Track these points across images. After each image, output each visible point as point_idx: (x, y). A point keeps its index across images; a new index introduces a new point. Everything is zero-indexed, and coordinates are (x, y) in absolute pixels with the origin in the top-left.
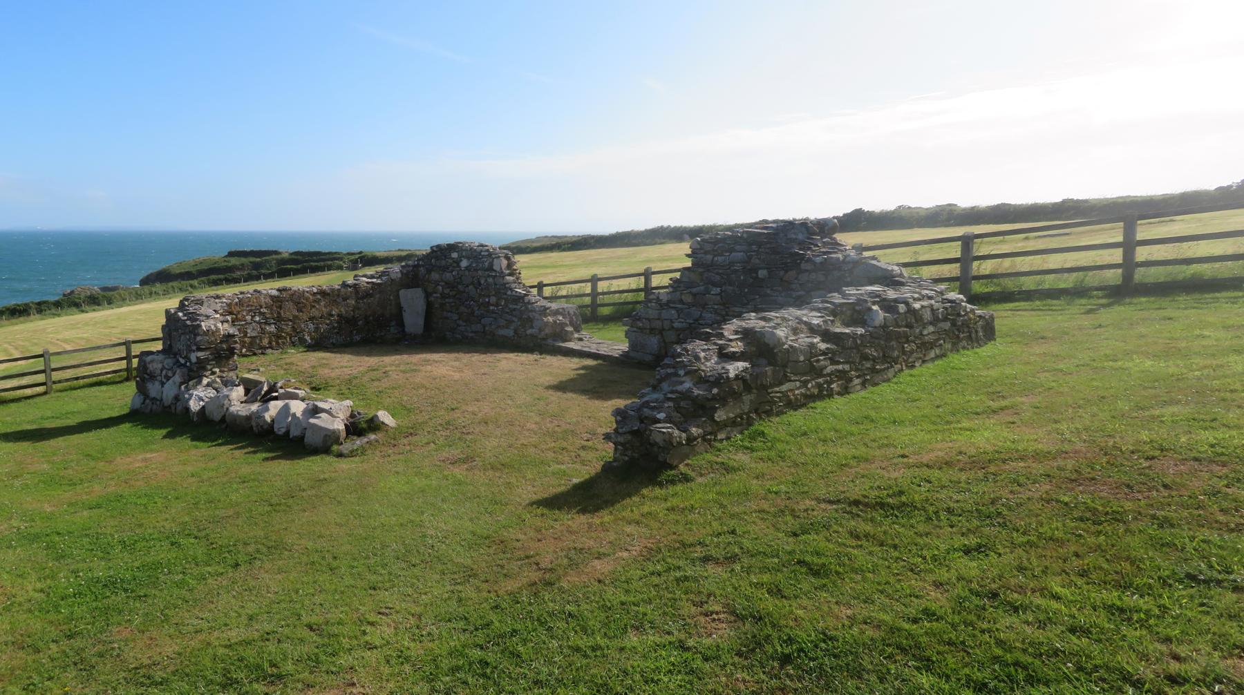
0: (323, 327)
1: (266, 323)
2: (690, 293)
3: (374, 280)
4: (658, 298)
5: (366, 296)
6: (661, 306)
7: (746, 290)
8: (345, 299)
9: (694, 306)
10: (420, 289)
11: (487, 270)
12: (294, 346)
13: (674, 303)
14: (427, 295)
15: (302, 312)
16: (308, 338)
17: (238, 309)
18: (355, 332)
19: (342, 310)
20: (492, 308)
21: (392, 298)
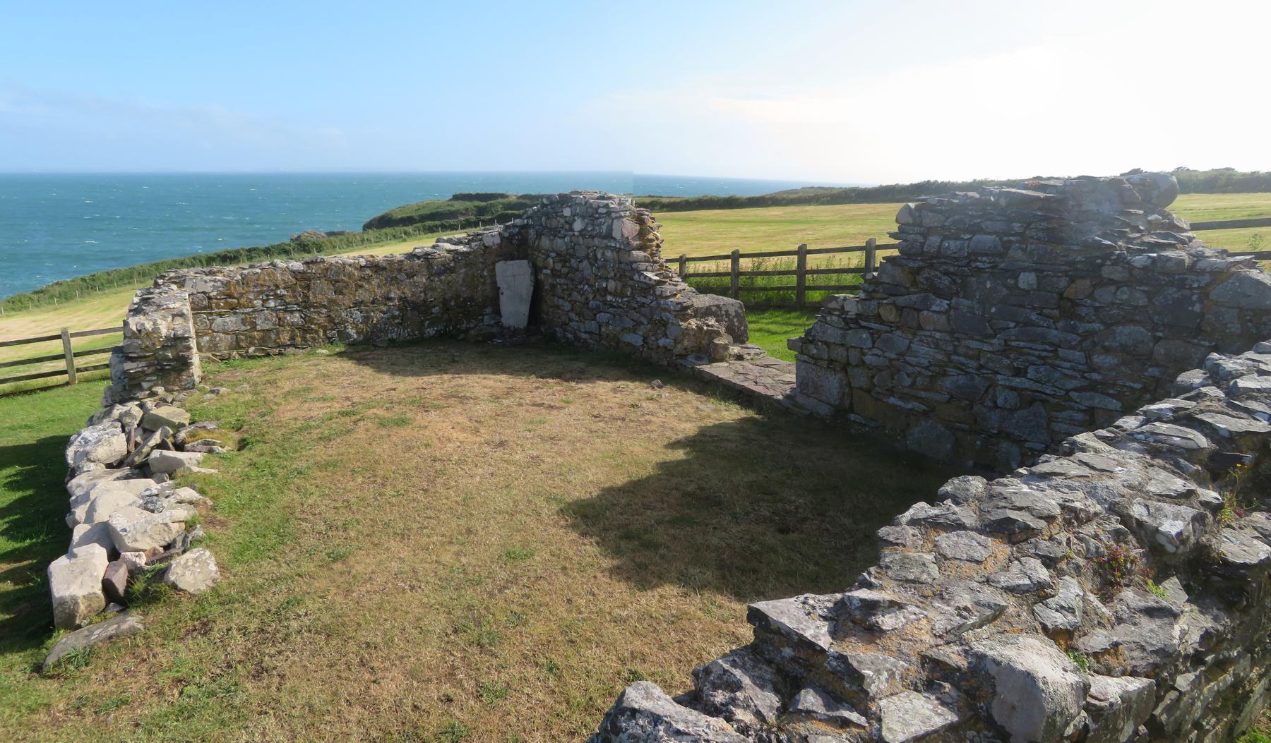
0: (376, 317)
1: (285, 311)
2: (894, 304)
4: (843, 307)
5: (445, 272)
6: (847, 324)
7: (993, 310)
8: (410, 276)
9: (898, 328)
10: (525, 262)
11: (605, 237)
12: (332, 343)
13: (867, 319)
14: (536, 270)
15: (341, 293)
16: (352, 331)
17: (240, 290)
19: (406, 290)
20: (609, 298)
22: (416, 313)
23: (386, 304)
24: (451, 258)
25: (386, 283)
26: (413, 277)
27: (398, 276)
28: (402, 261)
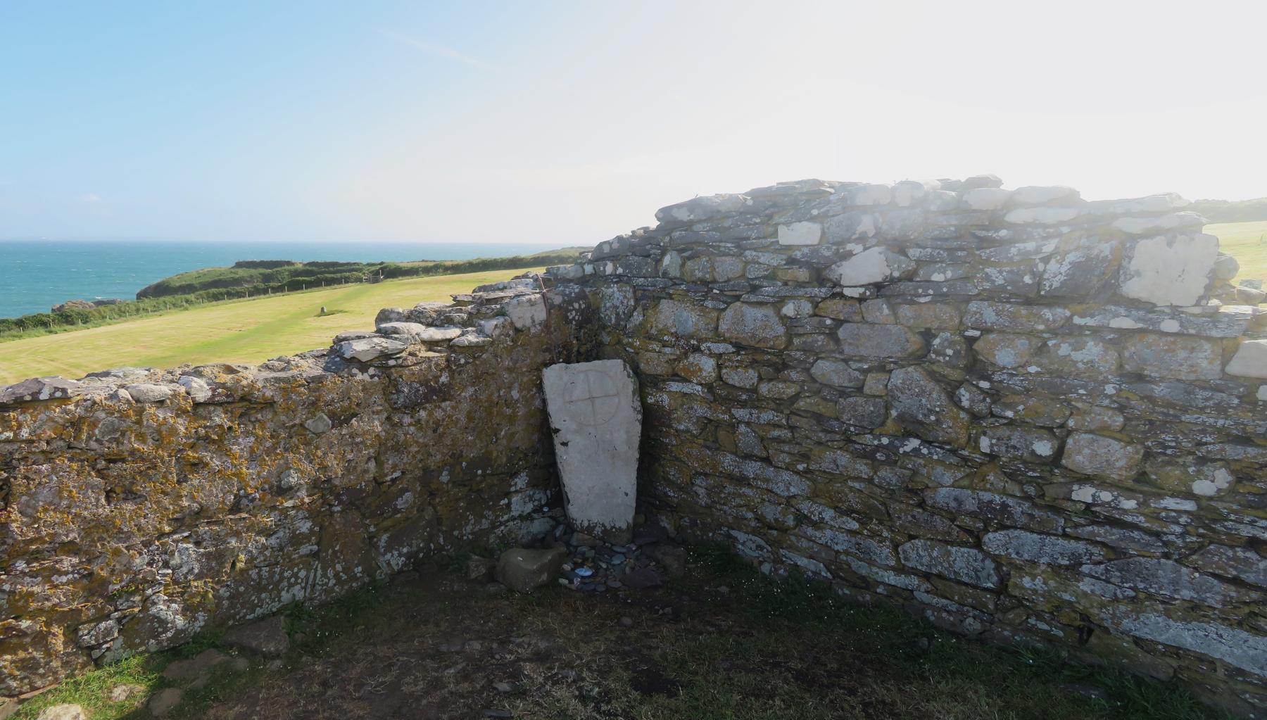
3: (453, 333)
5: (427, 398)
8: (339, 419)
15: (130, 495)
18: (385, 537)
19: (331, 461)
21: (515, 394)
22: (355, 516)
23: (274, 508)
24: (443, 363)
25: (274, 447)
26: (347, 421)
28: (319, 379)
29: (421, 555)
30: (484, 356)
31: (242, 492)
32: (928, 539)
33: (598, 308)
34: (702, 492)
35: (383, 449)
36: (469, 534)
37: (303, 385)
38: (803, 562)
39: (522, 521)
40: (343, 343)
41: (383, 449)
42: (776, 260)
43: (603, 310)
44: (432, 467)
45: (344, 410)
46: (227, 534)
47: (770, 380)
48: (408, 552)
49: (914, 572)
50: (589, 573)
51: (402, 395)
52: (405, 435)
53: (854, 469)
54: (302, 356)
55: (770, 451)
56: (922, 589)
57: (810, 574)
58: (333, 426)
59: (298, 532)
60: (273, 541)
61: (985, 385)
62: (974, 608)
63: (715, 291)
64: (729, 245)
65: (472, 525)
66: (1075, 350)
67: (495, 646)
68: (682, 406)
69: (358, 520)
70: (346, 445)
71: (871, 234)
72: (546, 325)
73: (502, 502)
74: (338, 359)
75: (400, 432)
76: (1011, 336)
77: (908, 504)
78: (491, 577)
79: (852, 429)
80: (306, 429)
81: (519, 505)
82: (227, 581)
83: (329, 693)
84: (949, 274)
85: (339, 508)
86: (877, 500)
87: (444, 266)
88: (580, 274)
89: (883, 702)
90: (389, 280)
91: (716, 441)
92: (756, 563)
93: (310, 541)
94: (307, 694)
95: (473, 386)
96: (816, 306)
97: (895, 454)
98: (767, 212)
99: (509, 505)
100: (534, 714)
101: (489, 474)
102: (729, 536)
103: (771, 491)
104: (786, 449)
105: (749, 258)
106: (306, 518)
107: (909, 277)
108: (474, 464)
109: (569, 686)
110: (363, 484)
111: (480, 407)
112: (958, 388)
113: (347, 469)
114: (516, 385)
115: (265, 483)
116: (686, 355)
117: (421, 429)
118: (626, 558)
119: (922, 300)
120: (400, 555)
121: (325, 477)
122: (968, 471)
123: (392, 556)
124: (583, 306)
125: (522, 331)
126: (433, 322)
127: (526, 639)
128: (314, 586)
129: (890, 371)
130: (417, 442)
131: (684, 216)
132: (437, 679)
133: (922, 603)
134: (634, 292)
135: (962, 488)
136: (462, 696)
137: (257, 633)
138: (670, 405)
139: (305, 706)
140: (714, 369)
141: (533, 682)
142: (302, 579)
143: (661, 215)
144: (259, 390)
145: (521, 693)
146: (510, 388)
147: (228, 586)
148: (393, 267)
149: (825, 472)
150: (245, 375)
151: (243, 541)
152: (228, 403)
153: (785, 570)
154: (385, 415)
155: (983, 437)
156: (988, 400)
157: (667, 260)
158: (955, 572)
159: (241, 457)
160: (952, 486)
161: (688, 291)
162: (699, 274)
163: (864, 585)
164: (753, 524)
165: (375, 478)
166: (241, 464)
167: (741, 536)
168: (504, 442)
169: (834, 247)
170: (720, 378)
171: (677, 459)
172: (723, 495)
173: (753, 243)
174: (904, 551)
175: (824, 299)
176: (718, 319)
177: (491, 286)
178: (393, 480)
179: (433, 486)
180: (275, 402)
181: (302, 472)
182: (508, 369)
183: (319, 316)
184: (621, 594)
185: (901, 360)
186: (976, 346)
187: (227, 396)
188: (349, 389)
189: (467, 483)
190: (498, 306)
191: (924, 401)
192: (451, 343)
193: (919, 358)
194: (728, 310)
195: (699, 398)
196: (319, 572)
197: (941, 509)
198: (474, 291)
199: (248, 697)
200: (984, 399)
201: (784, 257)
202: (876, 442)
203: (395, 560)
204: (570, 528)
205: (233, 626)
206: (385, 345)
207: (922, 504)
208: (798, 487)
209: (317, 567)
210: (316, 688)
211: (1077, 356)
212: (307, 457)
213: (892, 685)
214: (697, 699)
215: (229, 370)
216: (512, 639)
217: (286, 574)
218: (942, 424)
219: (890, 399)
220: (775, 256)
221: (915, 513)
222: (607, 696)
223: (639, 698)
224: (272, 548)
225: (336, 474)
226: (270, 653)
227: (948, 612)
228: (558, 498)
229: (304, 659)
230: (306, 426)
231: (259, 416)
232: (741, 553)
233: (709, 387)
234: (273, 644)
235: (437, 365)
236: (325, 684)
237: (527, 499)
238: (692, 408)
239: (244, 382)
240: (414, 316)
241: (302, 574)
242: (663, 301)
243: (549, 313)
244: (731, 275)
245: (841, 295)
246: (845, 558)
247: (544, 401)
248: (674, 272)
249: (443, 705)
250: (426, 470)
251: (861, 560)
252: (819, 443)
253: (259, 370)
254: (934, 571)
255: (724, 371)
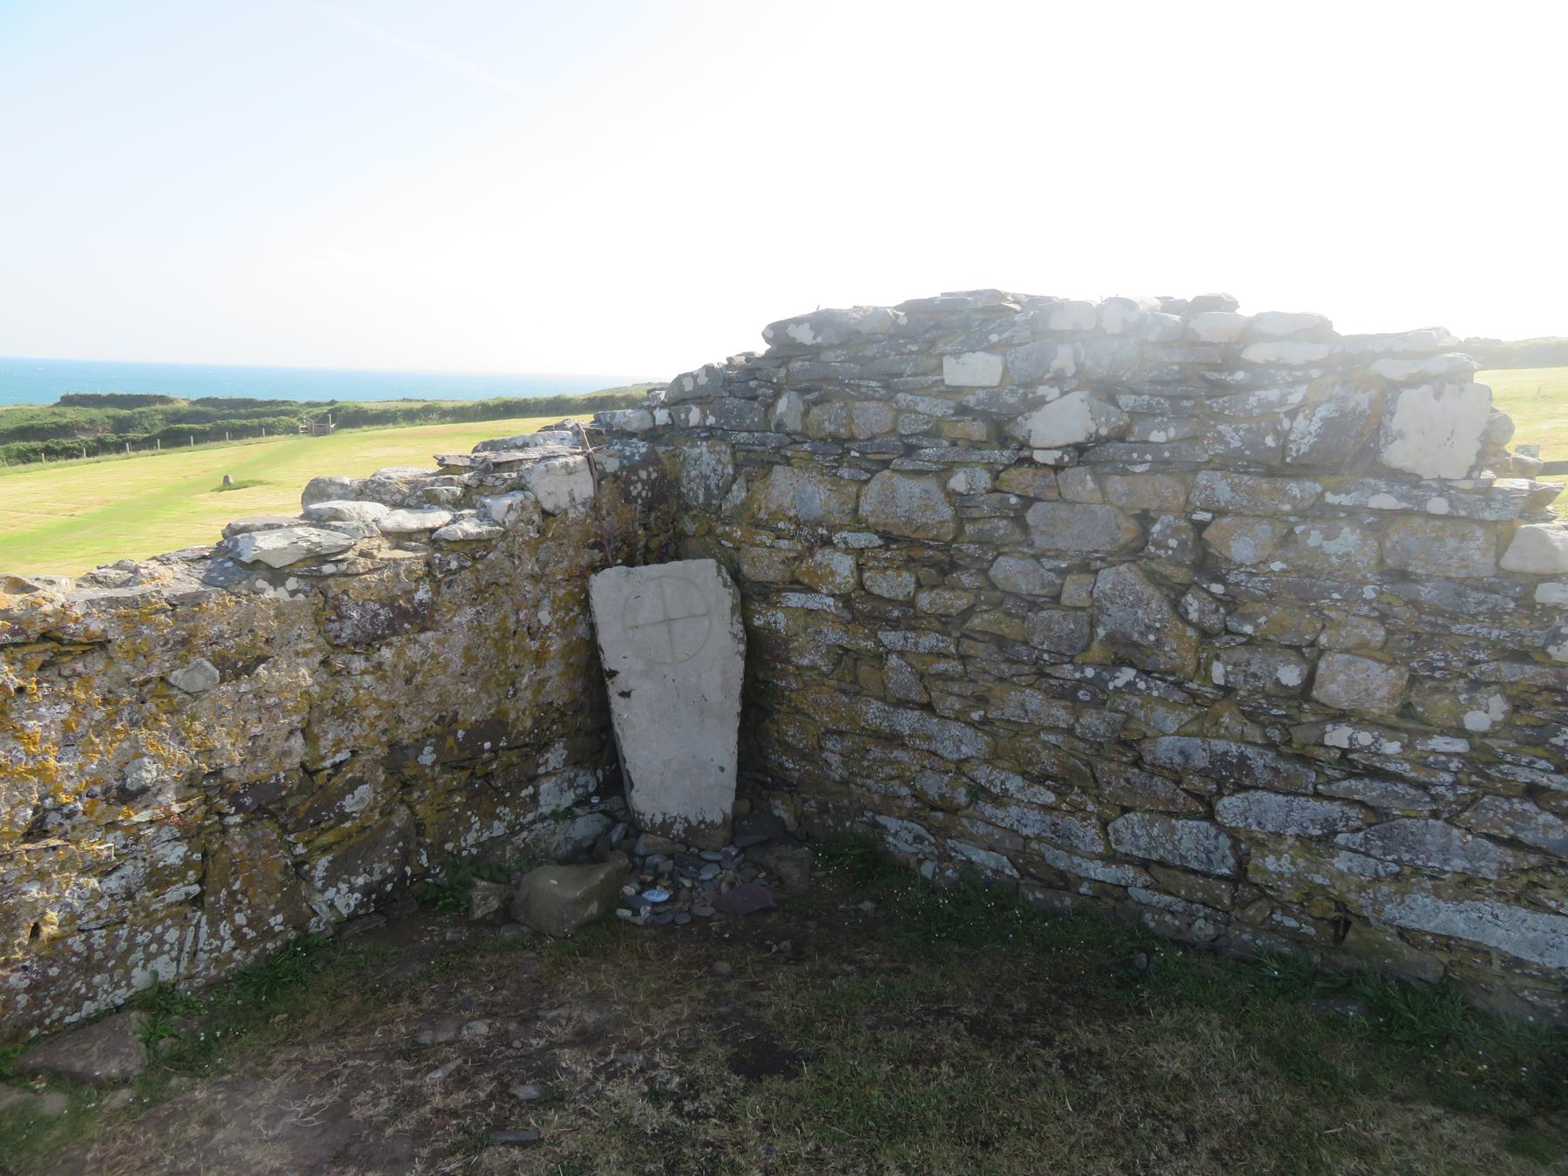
3: (437, 518)
5: (393, 628)
8: (235, 667)
18: (323, 862)
19: (221, 739)
21: (545, 617)
22: (269, 831)
23: (112, 826)
24: (420, 569)
25: (111, 720)
26: (249, 669)
27: (177, 676)
28: (194, 600)
29: (389, 887)
30: (491, 556)
31: (48, 802)
32: (1148, 811)
33: (677, 480)
34: (835, 759)
35: (316, 714)
36: (472, 846)
37: (165, 611)
38: (979, 856)
39: (556, 821)
40: (239, 537)
41: (316, 714)
42: (941, 408)
43: (685, 481)
44: (405, 742)
45: (242, 652)
46: (21, 878)
47: (933, 587)
48: (366, 884)
49: (1128, 859)
50: (664, 897)
51: (348, 623)
52: (355, 689)
53: (1049, 715)
54: (164, 560)
55: (933, 694)
56: (1139, 885)
57: (989, 873)
58: (223, 680)
59: (162, 863)
60: (113, 883)
61: (1217, 589)
62: (1205, 904)
63: (853, 453)
64: (873, 384)
65: (477, 831)
66: (1327, 538)
67: (512, 1026)
68: (805, 629)
69: (274, 837)
70: (248, 710)
71: (1070, 372)
72: (594, 506)
73: (524, 793)
74: (230, 564)
75: (346, 685)
76: (1250, 520)
77: (1120, 763)
78: (507, 914)
79: (1046, 657)
80: (173, 686)
81: (552, 796)
82: (24, 961)
83: (220, 1135)
84: (1172, 432)
85: (237, 819)
86: (1080, 759)
87: (440, 408)
88: (648, 425)
89: (1089, 1051)
90: (345, 430)
91: (855, 681)
92: (913, 863)
93: (184, 878)
94: (178, 1142)
95: (472, 605)
96: (996, 476)
97: (1103, 692)
98: (928, 336)
99: (534, 797)
100: (577, 1130)
101: (503, 748)
102: (875, 825)
103: (935, 753)
104: (956, 689)
105: (903, 404)
106: (177, 839)
107: (1120, 436)
108: (477, 732)
109: (633, 1078)
110: (282, 775)
111: (486, 639)
112: (1184, 594)
113: (252, 752)
114: (546, 602)
115: (94, 783)
116: (810, 550)
117: (384, 678)
118: (722, 869)
119: (1138, 469)
120: (352, 890)
121: (209, 767)
122: (1197, 711)
123: (338, 891)
124: (654, 475)
125: (554, 516)
126: (403, 501)
127: (563, 1012)
128: (195, 954)
129: (1096, 572)
130: (376, 701)
131: (805, 336)
132: (412, 1090)
133: (1139, 903)
134: (734, 454)
135: (1190, 735)
136: (454, 1114)
137: (85, 1046)
138: (787, 627)
139: (174, 1164)
140: (852, 572)
141: (575, 1079)
142: (172, 945)
143: (771, 334)
144: (76, 621)
145: (555, 1099)
146: (536, 606)
147: (25, 968)
148: (351, 410)
149: (1009, 721)
150: (48, 595)
151: (54, 888)
152: (16, 645)
153: (955, 871)
154: (320, 657)
155: (1215, 663)
156: (1222, 610)
157: (782, 405)
158: (1181, 856)
159: (44, 740)
160: (1177, 733)
161: (814, 453)
162: (830, 428)
163: (1062, 884)
164: (909, 804)
165: (303, 765)
166: (46, 752)
167: (891, 823)
168: (528, 694)
169: (1021, 391)
170: (861, 585)
171: (798, 711)
172: (866, 763)
173: (907, 382)
174: (1116, 831)
175: (1007, 467)
176: (858, 497)
177: (504, 441)
178: (337, 767)
179: (407, 772)
180: (110, 641)
181: (166, 761)
182: (532, 576)
183: (221, 490)
184: (714, 926)
185: (1111, 556)
186: (1208, 534)
187: (14, 633)
188: (250, 615)
189: (466, 764)
190: (514, 475)
191: (1140, 612)
192: (434, 536)
193: (1134, 552)
194: (873, 482)
195: (830, 617)
196: (204, 929)
197: (1164, 768)
198: (475, 450)
199: (65, 1161)
200: (1217, 610)
201: (952, 404)
202: (1078, 675)
203: (344, 899)
204: (635, 827)
205: (38, 1037)
206: (315, 539)
207: (1138, 762)
208: (972, 745)
209: (199, 922)
210: (195, 1130)
211: (1330, 547)
212: (175, 733)
213: (1100, 1026)
214: (829, 1078)
215: (18, 586)
216: (540, 1013)
217: (140, 939)
218: (1164, 645)
219: (1096, 612)
220: (939, 401)
221: (1129, 775)
222: (692, 1087)
223: (742, 1085)
224: (112, 896)
225: (230, 760)
226: (110, 1079)
227: (1172, 913)
228: (615, 782)
229: (174, 1082)
230: (171, 680)
231: (79, 667)
232: (892, 849)
233: (846, 600)
234: (117, 1061)
235: (410, 571)
236: (212, 1122)
237: (565, 785)
238: (821, 632)
239: (48, 608)
240: (366, 491)
241: (172, 935)
242: (777, 468)
243: (598, 485)
244: (876, 430)
245: (1030, 461)
246: (1037, 847)
247: (592, 627)
248: (793, 424)
249: (421, 1134)
250: (393, 745)
251: (1057, 847)
252: (1001, 679)
253: (79, 586)
254: (1155, 857)
255: (867, 575)
